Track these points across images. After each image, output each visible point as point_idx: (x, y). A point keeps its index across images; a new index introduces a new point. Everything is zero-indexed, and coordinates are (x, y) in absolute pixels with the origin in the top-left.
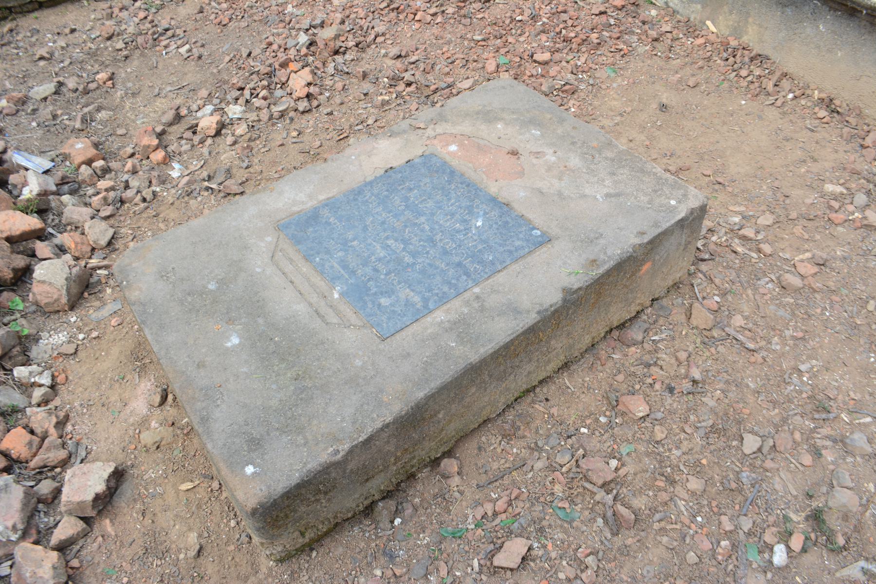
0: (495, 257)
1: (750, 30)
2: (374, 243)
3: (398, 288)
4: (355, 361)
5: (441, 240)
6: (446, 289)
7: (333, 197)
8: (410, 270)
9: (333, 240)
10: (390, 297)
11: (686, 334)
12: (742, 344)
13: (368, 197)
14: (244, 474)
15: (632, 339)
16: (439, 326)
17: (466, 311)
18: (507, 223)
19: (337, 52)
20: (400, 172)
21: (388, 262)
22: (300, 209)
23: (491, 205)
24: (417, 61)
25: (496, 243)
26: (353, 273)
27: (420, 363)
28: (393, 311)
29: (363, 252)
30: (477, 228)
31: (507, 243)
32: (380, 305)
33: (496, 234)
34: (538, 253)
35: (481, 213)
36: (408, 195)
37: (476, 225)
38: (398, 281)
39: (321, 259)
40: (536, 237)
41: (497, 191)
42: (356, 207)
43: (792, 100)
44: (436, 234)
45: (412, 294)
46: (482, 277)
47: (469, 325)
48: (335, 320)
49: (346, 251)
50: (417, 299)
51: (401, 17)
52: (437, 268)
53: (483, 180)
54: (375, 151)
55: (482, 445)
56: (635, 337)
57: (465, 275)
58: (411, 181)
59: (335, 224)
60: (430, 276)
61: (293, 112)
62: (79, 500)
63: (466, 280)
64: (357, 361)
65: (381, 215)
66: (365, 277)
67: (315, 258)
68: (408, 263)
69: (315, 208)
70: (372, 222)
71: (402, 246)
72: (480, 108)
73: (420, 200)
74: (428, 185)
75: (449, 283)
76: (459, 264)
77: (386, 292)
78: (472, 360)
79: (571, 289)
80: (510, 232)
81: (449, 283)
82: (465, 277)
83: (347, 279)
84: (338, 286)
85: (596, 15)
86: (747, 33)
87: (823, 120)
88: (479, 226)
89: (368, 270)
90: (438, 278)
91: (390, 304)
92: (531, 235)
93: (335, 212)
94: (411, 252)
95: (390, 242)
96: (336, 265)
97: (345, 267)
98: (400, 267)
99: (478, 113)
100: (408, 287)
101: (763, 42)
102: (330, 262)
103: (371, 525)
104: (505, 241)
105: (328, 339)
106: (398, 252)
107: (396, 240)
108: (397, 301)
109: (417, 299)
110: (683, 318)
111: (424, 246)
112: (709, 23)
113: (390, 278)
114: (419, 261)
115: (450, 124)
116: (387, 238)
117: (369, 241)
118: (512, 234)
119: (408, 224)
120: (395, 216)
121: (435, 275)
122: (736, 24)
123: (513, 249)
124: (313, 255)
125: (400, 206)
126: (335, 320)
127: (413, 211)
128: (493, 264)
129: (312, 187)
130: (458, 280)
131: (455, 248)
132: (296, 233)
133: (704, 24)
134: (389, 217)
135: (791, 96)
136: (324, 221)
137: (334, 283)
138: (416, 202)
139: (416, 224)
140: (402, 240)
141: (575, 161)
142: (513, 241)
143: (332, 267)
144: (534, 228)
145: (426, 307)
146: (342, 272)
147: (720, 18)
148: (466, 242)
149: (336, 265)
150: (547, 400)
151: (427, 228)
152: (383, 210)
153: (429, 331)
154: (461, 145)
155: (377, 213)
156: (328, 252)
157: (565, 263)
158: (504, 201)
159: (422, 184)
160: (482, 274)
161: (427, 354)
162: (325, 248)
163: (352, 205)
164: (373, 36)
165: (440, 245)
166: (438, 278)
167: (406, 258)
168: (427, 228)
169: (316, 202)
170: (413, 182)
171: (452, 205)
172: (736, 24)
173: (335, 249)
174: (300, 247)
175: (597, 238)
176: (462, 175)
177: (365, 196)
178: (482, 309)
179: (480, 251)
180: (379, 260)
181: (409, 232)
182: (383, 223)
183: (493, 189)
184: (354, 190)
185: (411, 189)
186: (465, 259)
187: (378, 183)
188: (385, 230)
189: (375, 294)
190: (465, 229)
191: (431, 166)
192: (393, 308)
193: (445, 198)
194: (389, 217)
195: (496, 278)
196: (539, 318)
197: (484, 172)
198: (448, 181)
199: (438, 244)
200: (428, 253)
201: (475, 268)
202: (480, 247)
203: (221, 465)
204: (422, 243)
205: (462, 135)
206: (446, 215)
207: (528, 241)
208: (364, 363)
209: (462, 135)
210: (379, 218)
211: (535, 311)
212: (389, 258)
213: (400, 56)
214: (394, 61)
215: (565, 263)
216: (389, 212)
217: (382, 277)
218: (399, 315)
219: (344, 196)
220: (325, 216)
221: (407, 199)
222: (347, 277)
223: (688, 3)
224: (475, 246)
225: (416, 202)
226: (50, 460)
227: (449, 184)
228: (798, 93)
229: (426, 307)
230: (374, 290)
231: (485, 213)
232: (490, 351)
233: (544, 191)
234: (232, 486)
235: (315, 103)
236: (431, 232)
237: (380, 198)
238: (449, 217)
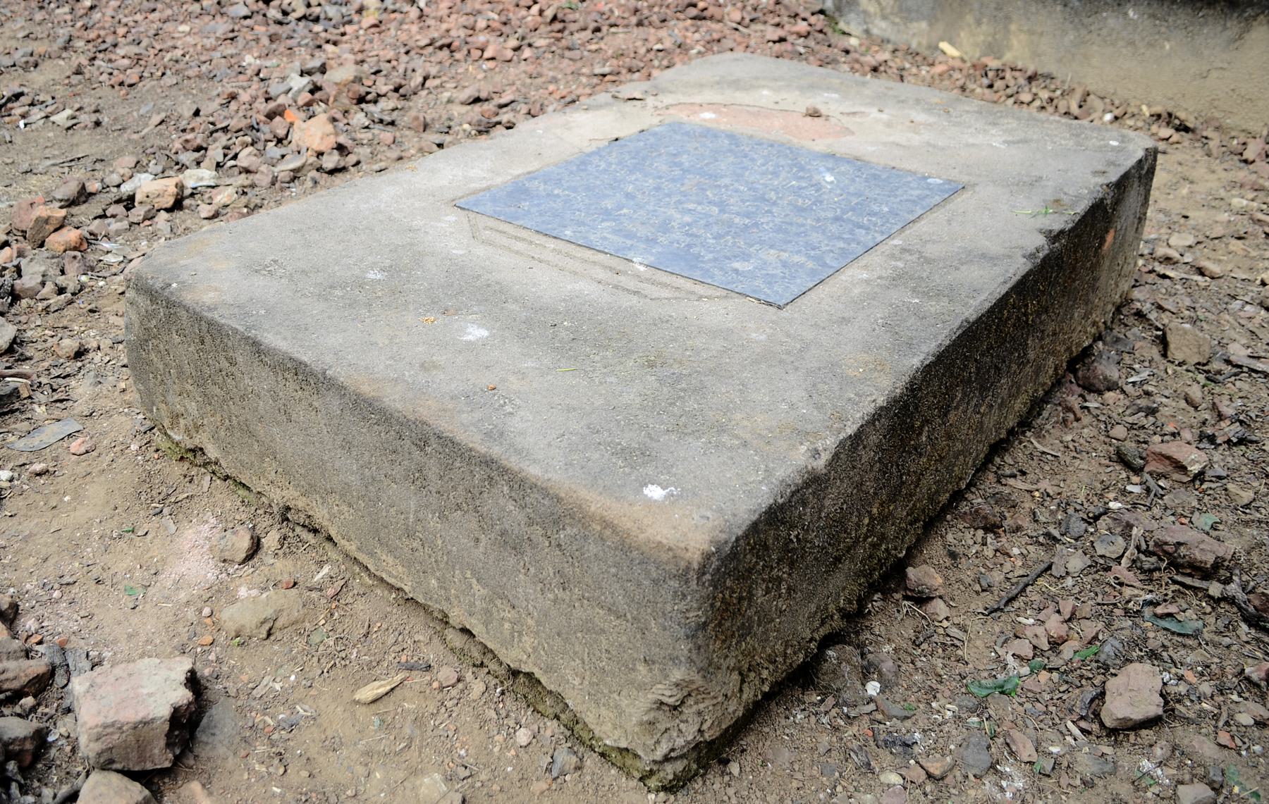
1: (1015, 42)
6: (841, 245)
11: (1175, 372)
14: (649, 503)
15: (1105, 378)
19: (361, 100)
20: (638, 141)
24: (512, 102)
43: (1111, 122)
49: (614, 220)
51: (457, 55)
52: (803, 225)
55: (953, 549)
56: (1108, 373)
61: (315, 172)
62: (139, 718)
72: (718, 78)
76: (837, 219)
78: (967, 314)
79: (1051, 231)
81: (839, 238)
85: (774, 42)
86: (1009, 48)
87: (1171, 140)
89: (677, 235)
95: (691, 206)
96: (608, 236)
97: (630, 236)
99: (718, 83)
101: (1039, 56)
103: (822, 701)
105: (671, 316)
110: (1155, 352)
112: (944, 46)
122: (990, 39)
126: (665, 293)
133: (937, 48)
135: (1108, 117)
141: (921, 117)
143: (605, 239)
147: (962, 34)
150: (1023, 473)
164: (420, 79)
172: (990, 39)
178: (928, 261)
182: (658, 189)
183: (820, 146)
184: (568, 163)
196: (1029, 266)
198: (731, 144)
203: (583, 493)
213: (477, 100)
214: (469, 107)
221: (680, 165)
223: (905, 24)
226: (9, 675)
228: (1118, 112)
230: (710, 256)
232: (987, 305)
234: (629, 525)
235: (352, 159)
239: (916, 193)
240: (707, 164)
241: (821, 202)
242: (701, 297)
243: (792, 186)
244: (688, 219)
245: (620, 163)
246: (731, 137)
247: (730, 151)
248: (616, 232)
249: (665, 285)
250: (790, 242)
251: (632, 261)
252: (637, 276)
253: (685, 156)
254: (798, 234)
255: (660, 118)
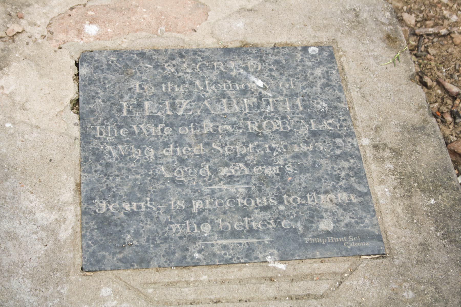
0: (325, 100)
2: (213, 187)
3: (309, 202)
4: (403, 296)
5: (260, 127)
6: (346, 165)
7: (78, 185)
8: (290, 179)
9: (171, 223)
10: (322, 217)
12: (437, 35)
13: (114, 153)
16: (397, 199)
17: (392, 167)
18: (277, 62)
20: (93, 98)
21: (260, 190)
22: (70, 231)
23: (236, 57)
25: (303, 88)
26: (251, 231)
27: (443, 242)
28: (347, 225)
29: (220, 204)
30: (265, 88)
31: (311, 79)
32: (328, 233)
33: (288, 80)
34: (346, 67)
35: (242, 71)
36: (147, 113)
37: (257, 86)
38: (301, 197)
39: (199, 252)
40: (319, 54)
41: (215, 40)
42: (124, 171)
44: (247, 127)
45: (332, 196)
46: (349, 127)
47: (411, 174)
48: (323, 287)
49: (205, 220)
50: (343, 196)
52: (305, 154)
53: (184, 40)
54: (18, 99)
57: (334, 138)
58: (122, 97)
59: (139, 207)
60: (314, 167)
63: (344, 141)
64: (405, 294)
65: (164, 156)
66: (269, 223)
67: (193, 258)
68: (277, 175)
69: (84, 213)
70: (171, 170)
71: (241, 165)
73: (167, 108)
74: (146, 88)
75: (338, 157)
77: (312, 217)
80: (295, 68)
82: (338, 140)
83: (259, 243)
84: (264, 257)
88: (264, 85)
89: (258, 215)
90: (323, 161)
91: (334, 223)
92: (313, 56)
93: (114, 196)
94: (259, 162)
95: (224, 171)
96: (225, 242)
97: (235, 234)
98: (278, 185)
100: (318, 193)
102: (213, 245)
104: (306, 79)
106: (247, 172)
107: (227, 165)
108: (334, 214)
109: (343, 196)
111: (258, 146)
113: (289, 202)
114: (281, 161)
115: (36, 6)
116: (214, 171)
117: (206, 190)
118: (300, 68)
119: (206, 140)
120: (179, 143)
121: (315, 162)
123: (323, 81)
124: (185, 257)
125: (162, 130)
127: (183, 125)
128: (336, 108)
129: (32, 197)
130: (338, 147)
131: (284, 123)
132: (120, 256)
134: (175, 152)
136: (122, 215)
137: (257, 258)
138: (169, 113)
139: (210, 134)
140: (230, 160)
142: (312, 74)
143: (225, 247)
144: (305, 49)
145: (360, 194)
146: (241, 241)
148: (280, 109)
149: (225, 242)
151: (229, 128)
152: (156, 149)
153: (399, 210)
154: (93, 21)
155: (156, 157)
156: (193, 239)
157: (376, 58)
158: (238, 45)
159: (138, 91)
160: (344, 124)
161: (432, 228)
162: (181, 238)
163: (116, 173)
165: (267, 132)
166: (323, 161)
167: (266, 171)
168: (229, 128)
169: (72, 208)
170: (127, 97)
171: (205, 87)
173: (192, 230)
174: (154, 263)
175: (357, 16)
176: (157, 51)
177: (110, 153)
178: (397, 153)
179: (305, 107)
180: (249, 196)
181: (222, 147)
184: (86, 159)
185: (140, 106)
186: (310, 125)
187: (95, 129)
188: (198, 166)
189: (306, 228)
190: (260, 97)
191: (108, 65)
192: (343, 224)
193: (186, 86)
194: (175, 152)
195: (358, 118)
197: (166, 31)
198: (156, 67)
199: (265, 133)
200: (272, 149)
201: (330, 124)
202: (298, 102)
204: (250, 146)
205: (72, 9)
206: (219, 101)
207: (320, 63)
208: (413, 290)
209: (72, 9)
210: (170, 160)
211: (427, 115)
212: (253, 188)
215: (376, 58)
216: (166, 145)
217: (282, 208)
218: (357, 223)
219: (89, 172)
220: (112, 210)
222: (255, 241)
224: (294, 106)
225: (169, 113)
227: (164, 69)
229: (360, 194)
230: (299, 226)
231: (246, 69)
233: (250, 7)
236: (240, 128)
237: (128, 142)
238: (224, 101)
239: (318, 72)
240: (173, 106)
241: (286, 118)
242: (342, 274)
243: (249, 106)
244: (241, 189)
245: (119, 140)
246: (142, 54)
247: (166, 78)
248: (222, 233)
249: (310, 277)
250: (319, 180)
251: (266, 262)
252: (285, 275)
253: (147, 104)
254: (314, 167)
255: (64, 52)
